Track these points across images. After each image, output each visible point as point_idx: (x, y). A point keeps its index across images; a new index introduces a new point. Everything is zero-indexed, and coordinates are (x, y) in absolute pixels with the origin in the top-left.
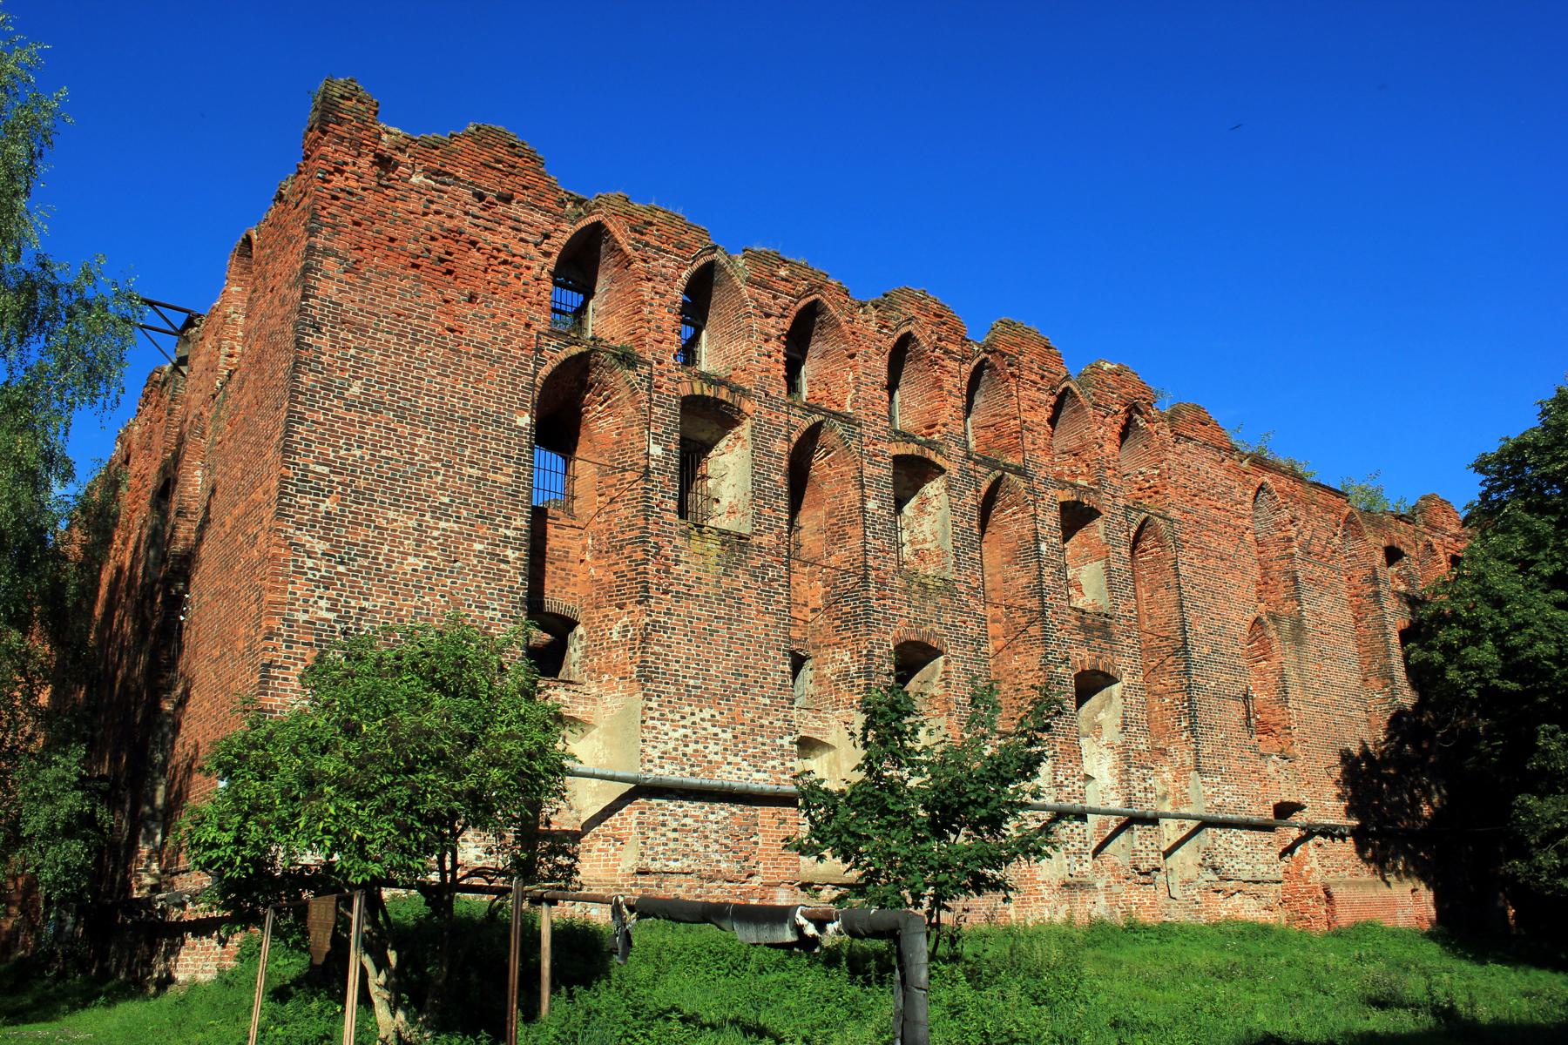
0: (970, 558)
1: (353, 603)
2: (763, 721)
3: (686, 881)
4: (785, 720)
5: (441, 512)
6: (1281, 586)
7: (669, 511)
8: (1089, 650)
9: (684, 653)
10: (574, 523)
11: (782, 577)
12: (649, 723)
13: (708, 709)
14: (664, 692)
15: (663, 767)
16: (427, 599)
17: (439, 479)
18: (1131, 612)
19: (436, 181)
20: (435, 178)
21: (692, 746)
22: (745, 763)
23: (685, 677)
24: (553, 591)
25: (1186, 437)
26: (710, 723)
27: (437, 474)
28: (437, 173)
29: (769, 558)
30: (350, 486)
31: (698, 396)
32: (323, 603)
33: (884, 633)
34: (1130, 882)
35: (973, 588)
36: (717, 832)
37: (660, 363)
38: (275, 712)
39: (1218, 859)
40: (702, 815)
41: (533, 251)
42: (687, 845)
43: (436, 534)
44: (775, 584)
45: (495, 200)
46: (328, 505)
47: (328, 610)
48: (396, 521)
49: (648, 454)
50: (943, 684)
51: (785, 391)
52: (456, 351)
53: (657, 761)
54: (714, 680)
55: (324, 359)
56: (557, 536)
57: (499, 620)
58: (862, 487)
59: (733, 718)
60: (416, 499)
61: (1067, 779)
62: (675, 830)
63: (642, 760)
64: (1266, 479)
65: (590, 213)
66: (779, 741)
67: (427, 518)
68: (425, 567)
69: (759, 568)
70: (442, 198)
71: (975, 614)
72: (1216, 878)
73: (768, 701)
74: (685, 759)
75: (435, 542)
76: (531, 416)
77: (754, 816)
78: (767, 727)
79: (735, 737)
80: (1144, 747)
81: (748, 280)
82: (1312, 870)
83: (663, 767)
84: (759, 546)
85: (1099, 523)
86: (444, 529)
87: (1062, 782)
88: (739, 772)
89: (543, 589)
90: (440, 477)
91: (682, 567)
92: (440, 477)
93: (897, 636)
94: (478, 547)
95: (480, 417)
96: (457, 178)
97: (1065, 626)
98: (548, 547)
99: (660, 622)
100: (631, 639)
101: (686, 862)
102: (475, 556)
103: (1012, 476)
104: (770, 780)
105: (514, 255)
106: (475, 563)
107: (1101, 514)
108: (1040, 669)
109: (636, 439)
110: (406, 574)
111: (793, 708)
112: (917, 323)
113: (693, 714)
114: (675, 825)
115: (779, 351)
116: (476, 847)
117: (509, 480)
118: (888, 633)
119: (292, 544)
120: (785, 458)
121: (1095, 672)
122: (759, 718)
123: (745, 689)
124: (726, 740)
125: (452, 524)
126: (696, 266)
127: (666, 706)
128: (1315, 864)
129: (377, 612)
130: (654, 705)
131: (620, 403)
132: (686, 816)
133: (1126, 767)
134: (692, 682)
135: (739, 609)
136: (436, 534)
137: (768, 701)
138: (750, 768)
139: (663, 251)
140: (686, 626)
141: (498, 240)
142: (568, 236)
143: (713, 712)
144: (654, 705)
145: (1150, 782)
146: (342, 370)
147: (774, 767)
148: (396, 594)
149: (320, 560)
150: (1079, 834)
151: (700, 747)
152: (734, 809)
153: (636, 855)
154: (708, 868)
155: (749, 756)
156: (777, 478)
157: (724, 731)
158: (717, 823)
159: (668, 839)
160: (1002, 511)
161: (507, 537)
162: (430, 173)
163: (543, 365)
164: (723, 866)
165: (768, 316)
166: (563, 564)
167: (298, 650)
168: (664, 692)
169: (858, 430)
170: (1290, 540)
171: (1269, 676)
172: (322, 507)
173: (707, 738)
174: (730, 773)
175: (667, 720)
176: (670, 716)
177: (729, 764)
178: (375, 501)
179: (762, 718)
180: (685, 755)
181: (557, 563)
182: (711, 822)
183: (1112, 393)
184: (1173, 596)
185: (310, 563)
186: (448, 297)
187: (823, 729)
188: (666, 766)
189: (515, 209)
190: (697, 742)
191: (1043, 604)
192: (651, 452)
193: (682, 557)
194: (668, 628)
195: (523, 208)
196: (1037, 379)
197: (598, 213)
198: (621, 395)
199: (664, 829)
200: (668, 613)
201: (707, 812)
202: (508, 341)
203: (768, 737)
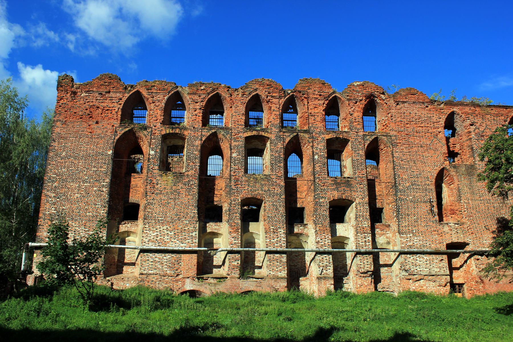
0: (278, 166)
1: (61, 208)
2: (185, 228)
3: (156, 276)
4: (194, 228)
5: (84, 181)
6: (467, 152)
7: (156, 169)
8: (338, 192)
9: (158, 210)
10: (140, 176)
11: (196, 183)
12: (145, 232)
13: (165, 226)
14: (150, 222)
15: (149, 244)
16: (80, 204)
17: (85, 173)
18: (364, 174)
19: (88, 94)
20: (88, 93)
21: (159, 237)
22: (178, 241)
23: (158, 217)
24: (132, 196)
25: (402, 102)
27: (85, 171)
28: (88, 91)
29: (191, 178)
30: (61, 179)
31: (168, 133)
32: (53, 209)
33: (236, 196)
34: (357, 276)
35: (279, 176)
36: (167, 262)
37: (155, 126)
38: (40, 236)
39: (408, 267)
40: (161, 257)
41: (116, 104)
42: (156, 266)
43: (83, 187)
44: (193, 186)
45: (105, 94)
46: (56, 184)
47: (54, 210)
48: (73, 185)
49: (149, 154)
51: (201, 125)
52: (91, 138)
53: (147, 242)
54: (168, 217)
55: (56, 148)
56: (134, 181)
57: (100, 207)
58: (231, 149)
59: (174, 228)
60: (79, 179)
61: (321, 240)
63: (142, 242)
64: (455, 110)
65: (134, 89)
66: (191, 234)
67: (81, 183)
68: (80, 196)
69: (187, 182)
70: (89, 98)
71: (279, 185)
72: (407, 274)
73: (188, 222)
74: (156, 241)
75: (83, 190)
76: (112, 151)
77: (180, 257)
78: (187, 230)
79: (175, 234)
80: (367, 225)
81: (188, 93)
82: (473, 270)
83: (149, 244)
84: (187, 175)
85: (350, 143)
86: (86, 186)
87: (319, 241)
88: (175, 244)
89: (129, 196)
90: (85, 172)
91: (159, 185)
92: (85, 172)
93: (242, 197)
94: (95, 189)
95: (97, 154)
96: (93, 91)
97: (325, 184)
98: (131, 184)
99: (150, 202)
101: (155, 271)
102: (94, 191)
103: (302, 134)
104: (187, 246)
105: (110, 107)
106: (94, 193)
107: (350, 140)
110: (75, 199)
111: (197, 224)
112: (259, 90)
113: (160, 228)
114: (152, 260)
115: (200, 113)
117: (105, 169)
118: (239, 196)
119: (46, 195)
120: (200, 146)
121: (340, 200)
122: (184, 227)
123: (179, 219)
124: (171, 235)
125: (88, 184)
126: (170, 94)
127: (151, 226)
128: (474, 267)
129: (67, 209)
130: (147, 226)
132: (156, 258)
134: (160, 219)
135: (179, 195)
136: (83, 187)
137: (188, 222)
138: (179, 243)
139: (158, 93)
140: (159, 202)
141: (105, 105)
142: (127, 97)
143: (167, 227)
144: (147, 226)
145: (368, 238)
146: (60, 150)
147: (189, 242)
148: (72, 204)
149: (53, 198)
150: (326, 259)
151: (162, 237)
152: (173, 255)
153: (139, 269)
154: (163, 273)
155: (180, 239)
156: (196, 153)
157: (170, 232)
158: (166, 259)
159: (150, 265)
160: (304, 146)
161: (103, 185)
162: (86, 92)
163: (117, 136)
164: (168, 272)
165: (197, 103)
166: (136, 189)
167: (46, 221)
168: (150, 222)
169: (230, 131)
170: (470, 132)
171: (454, 191)
172: (54, 185)
173: (164, 235)
174: (172, 244)
175: (151, 230)
176: (152, 229)
177: (172, 242)
178: (68, 181)
179: (185, 227)
180: (156, 240)
181: (134, 189)
182: (165, 259)
183: (359, 93)
184: (392, 165)
185: (50, 199)
186: (89, 124)
187: (218, 229)
188: (150, 244)
189: (112, 94)
190: (161, 236)
191: (314, 177)
192: (150, 153)
193: (159, 182)
194: (153, 204)
195: (113, 93)
196: (318, 96)
197: (137, 88)
199: (148, 261)
200: (153, 199)
202: (107, 132)
203: (187, 233)
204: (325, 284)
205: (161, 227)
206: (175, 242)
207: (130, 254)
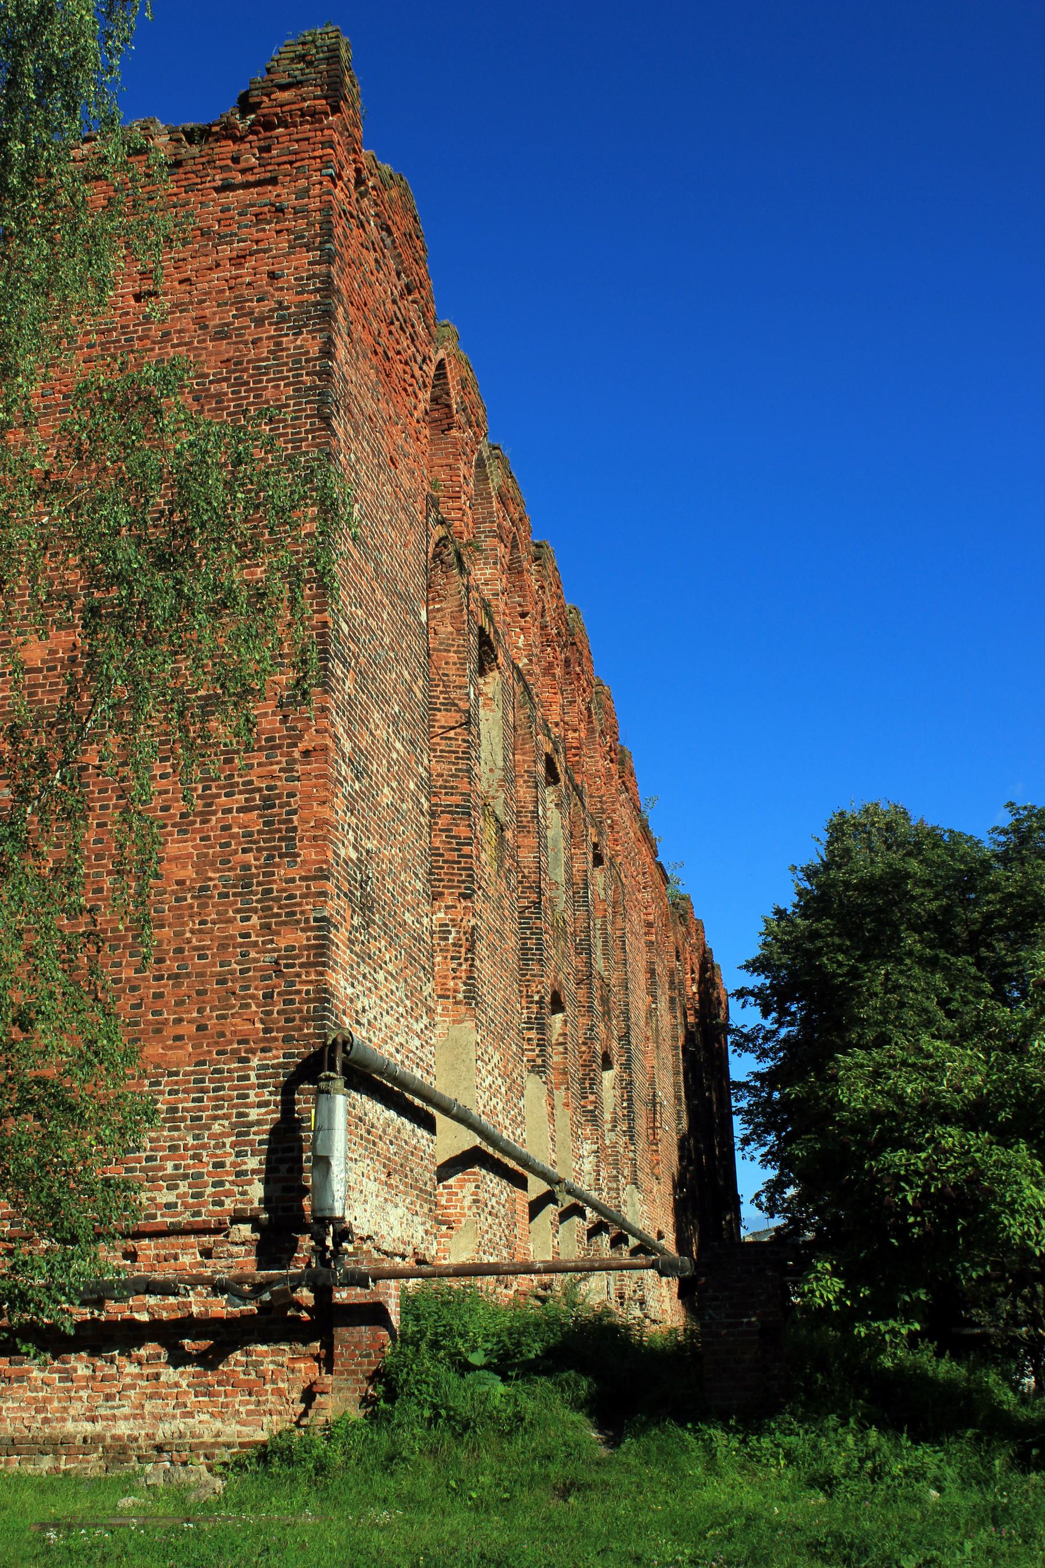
100: (454, 945)
108: (584, 1043)
109: (452, 670)
131: (439, 615)
198: (444, 605)
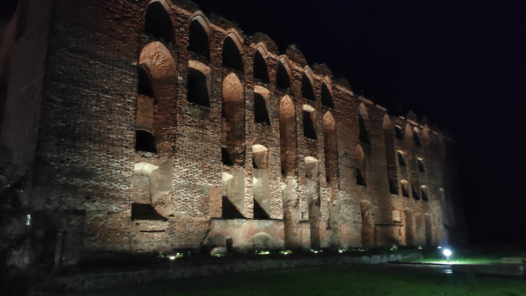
12: (176, 166)
16: (100, 121)
22: (206, 180)
26: (196, 167)
50: (267, 158)
53: (178, 179)
62: (183, 201)
88: (204, 183)
113: (190, 164)
114: (183, 199)
116: (116, 206)
130: (178, 160)
133: (318, 186)
157: (200, 170)
159: (181, 204)
174: (201, 183)
177: (201, 180)
180: (187, 177)
190: (191, 173)
201: (194, 196)
204: (305, 227)
205: (191, 163)
206: (204, 180)
207: (143, 192)
